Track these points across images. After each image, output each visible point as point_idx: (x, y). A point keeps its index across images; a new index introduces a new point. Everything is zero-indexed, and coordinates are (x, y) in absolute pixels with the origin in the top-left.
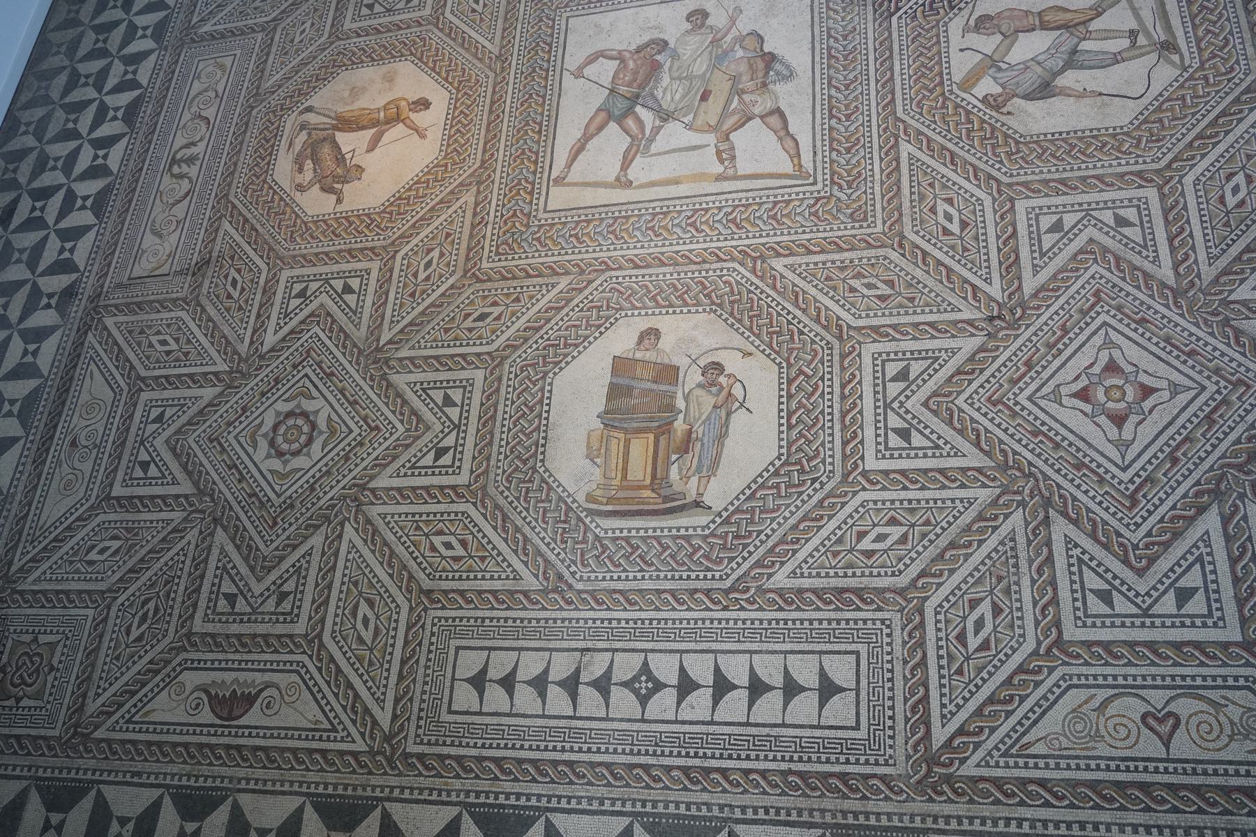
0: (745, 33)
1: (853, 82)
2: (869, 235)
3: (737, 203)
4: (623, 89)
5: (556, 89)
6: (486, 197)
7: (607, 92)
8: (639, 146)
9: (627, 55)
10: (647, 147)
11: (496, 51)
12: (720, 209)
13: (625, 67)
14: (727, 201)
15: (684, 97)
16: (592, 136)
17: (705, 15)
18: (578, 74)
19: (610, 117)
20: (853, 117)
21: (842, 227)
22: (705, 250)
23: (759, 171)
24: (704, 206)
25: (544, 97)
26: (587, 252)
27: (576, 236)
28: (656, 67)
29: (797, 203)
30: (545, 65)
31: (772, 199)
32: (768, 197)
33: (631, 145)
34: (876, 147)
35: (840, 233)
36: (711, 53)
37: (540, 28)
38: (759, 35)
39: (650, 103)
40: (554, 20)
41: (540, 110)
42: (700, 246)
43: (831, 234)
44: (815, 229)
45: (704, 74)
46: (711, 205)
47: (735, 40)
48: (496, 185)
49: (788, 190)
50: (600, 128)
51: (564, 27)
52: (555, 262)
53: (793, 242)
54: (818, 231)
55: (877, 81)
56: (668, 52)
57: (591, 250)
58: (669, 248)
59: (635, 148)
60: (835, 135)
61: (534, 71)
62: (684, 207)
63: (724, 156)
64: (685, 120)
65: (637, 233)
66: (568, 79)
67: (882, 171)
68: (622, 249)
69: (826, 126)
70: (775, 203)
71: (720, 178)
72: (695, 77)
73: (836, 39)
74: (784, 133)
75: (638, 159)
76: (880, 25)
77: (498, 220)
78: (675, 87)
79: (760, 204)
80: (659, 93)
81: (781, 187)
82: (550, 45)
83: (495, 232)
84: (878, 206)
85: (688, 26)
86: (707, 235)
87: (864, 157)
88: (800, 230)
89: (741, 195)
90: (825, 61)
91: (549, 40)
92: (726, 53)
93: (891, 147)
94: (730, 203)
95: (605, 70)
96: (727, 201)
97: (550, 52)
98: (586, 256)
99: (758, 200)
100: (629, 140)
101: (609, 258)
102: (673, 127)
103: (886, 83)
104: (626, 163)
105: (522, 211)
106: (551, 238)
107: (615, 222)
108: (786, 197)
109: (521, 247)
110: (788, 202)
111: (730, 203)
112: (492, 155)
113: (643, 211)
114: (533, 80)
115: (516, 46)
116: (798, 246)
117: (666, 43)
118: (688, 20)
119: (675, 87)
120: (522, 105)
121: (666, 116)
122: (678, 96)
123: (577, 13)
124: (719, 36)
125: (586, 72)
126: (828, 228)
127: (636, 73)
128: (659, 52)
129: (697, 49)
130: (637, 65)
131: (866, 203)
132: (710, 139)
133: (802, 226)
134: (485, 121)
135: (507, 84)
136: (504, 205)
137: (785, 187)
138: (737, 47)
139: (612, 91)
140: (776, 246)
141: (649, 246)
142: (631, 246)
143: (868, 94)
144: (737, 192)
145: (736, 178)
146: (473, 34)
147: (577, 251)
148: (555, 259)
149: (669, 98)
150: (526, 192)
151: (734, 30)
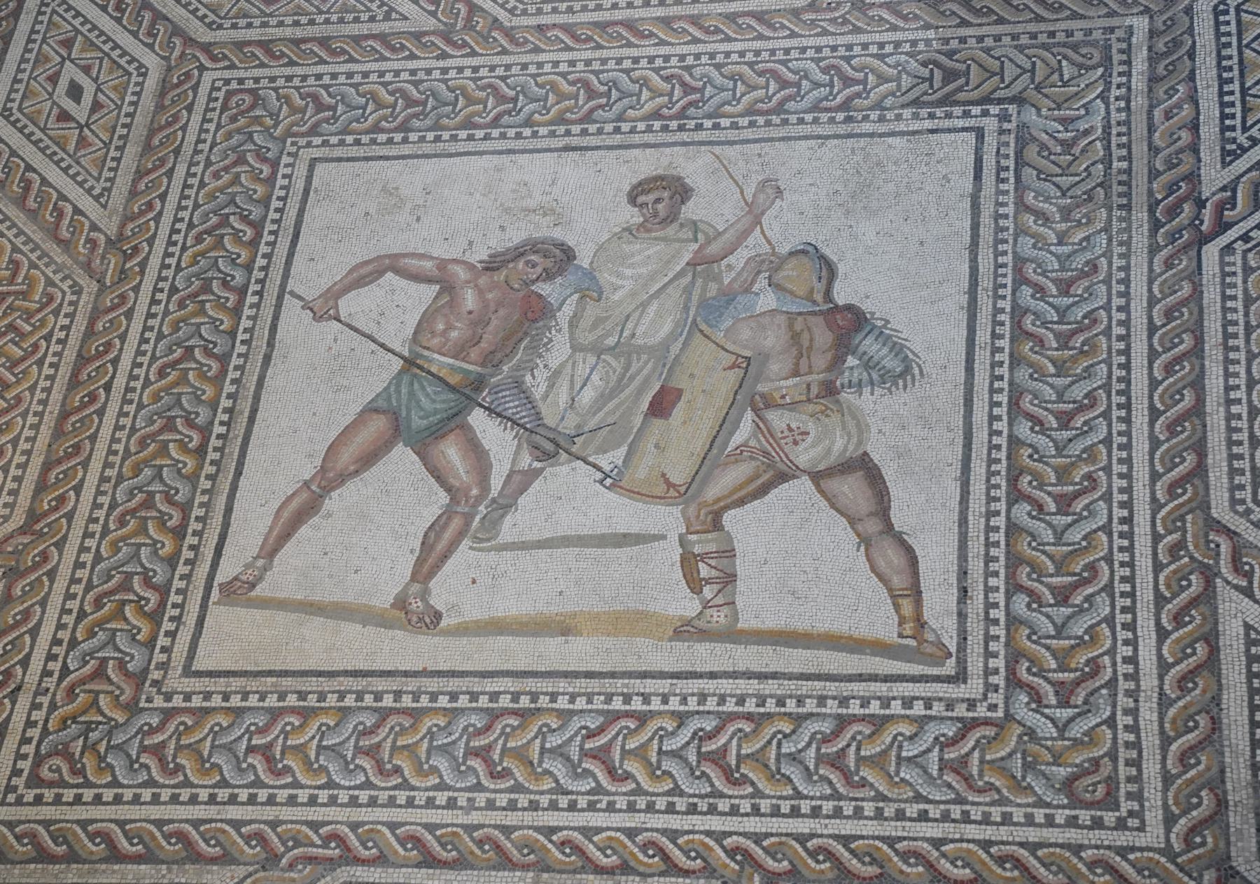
0: (784, 249)
1: (1081, 409)
2: (1123, 852)
3: (730, 706)
4: (440, 362)
5: (260, 344)
6: (27, 614)
7: (397, 364)
8: (468, 518)
9: (461, 273)
10: (492, 525)
11: (112, 231)
12: (681, 718)
13: (453, 304)
14: (703, 698)
15: (603, 398)
16: (343, 478)
17: (681, 191)
18: (324, 309)
19: (397, 431)
20: (1079, 505)
21: (1039, 815)
22: (631, 833)
23: (801, 625)
24: (637, 705)
25: (224, 360)
26: (292, 801)
27: (265, 751)
28: (535, 313)
29: (907, 730)
30: (239, 277)
31: (832, 707)
32: (822, 700)
33: (448, 514)
34: (1145, 595)
35: (1032, 835)
36: (688, 291)
37: (236, 180)
38: (823, 258)
39: (512, 406)
40: (275, 165)
41: (210, 392)
42: (616, 820)
43: (1003, 833)
44: (956, 811)
45: (665, 345)
46: (656, 704)
47: (758, 265)
48: (60, 585)
49: (882, 688)
50: (369, 459)
51: (300, 185)
52: (196, 824)
53: (891, 841)
54: (966, 819)
55: (1154, 414)
56: (571, 278)
57: (303, 795)
58: (528, 818)
59: (456, 523)
60: (1023, 546)
61: (206, 288)
62: (581, 703)
63: (704, 571)
64: (604, 462)
65: (442, 763)
66: (294, 318)
67: (1163, 667)
68: (392, 802)
69: (1000, 521)
70: (843, 722)
71: (686, 631)
72: (640, 350)
73: (1040, 290)
74: (877, 525)
75: (464, 554)
76: (1168, 265)
77: (50, 683)
78: (582, 370)
79: (799, 720)
80: (537, 383)
81: (860, 678)
82: (258, 226)
83: (38, 715)
84: (1151, 769)
85: (632, 216)
86: (639, 791)
87: (1110, 621)
88: (912, 810)
89: (742, 686)
90: (1004, 343)
91: (256, 213)
92: (728, 297)
93: (1193, 602)
94: (711, 705)
95: (398, 308)
96: (703, 698)
97: (254, 243)
98: (286, 813)
99: (791, 706)
100: (443, 497)
101: (354, 826)
102: (566, 477)
103: (1179, 420)
104: (429, 562)
105: (122, 665)
106: (194, 749)
107: (381, 724)
108: (875, 708)
109: (103, 766)
110: (879, 723)
111: (711, 705)
112: (62, 499)
113: (463, 701)
114: (202, 312)
115: (167, 220)
116: (905, 856)
117: (568, 254)
118: (632, 200)
119: (582, 370)
120: (162, 374)
121: (549, 446)
122: (588, 396)
123: (338, 152)
124: (714, 249)
125: (346, 306)
126: (996, 813)
127: (479, 321)
128: (548, 276)
129: (652, 277)
130: (485, 305)
131: (1113, 755)
132: (668, 519)
133: (919, 798)
134: (54, 408)
135: (129, 314)
136: (73, 643)
137: (874, 678)
138: (762, 282)
139: (410, 363)
140: (840, 849)
141: (472, 806)
142: (421, 798)
143: (1127, 447)
144: (734, 675)
145: (733, 635)
146: (54, 175)
147: (263, 795)
148: (198, 812)
149: (563, 399)
150: (140, 610)
151: (755, 237)
